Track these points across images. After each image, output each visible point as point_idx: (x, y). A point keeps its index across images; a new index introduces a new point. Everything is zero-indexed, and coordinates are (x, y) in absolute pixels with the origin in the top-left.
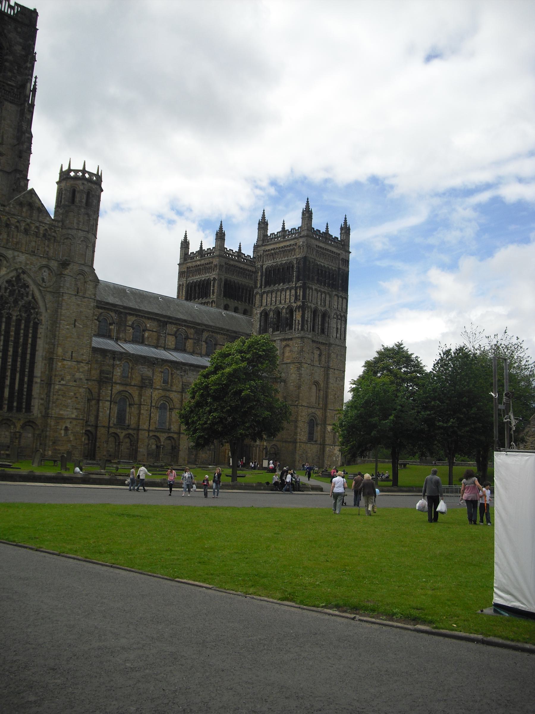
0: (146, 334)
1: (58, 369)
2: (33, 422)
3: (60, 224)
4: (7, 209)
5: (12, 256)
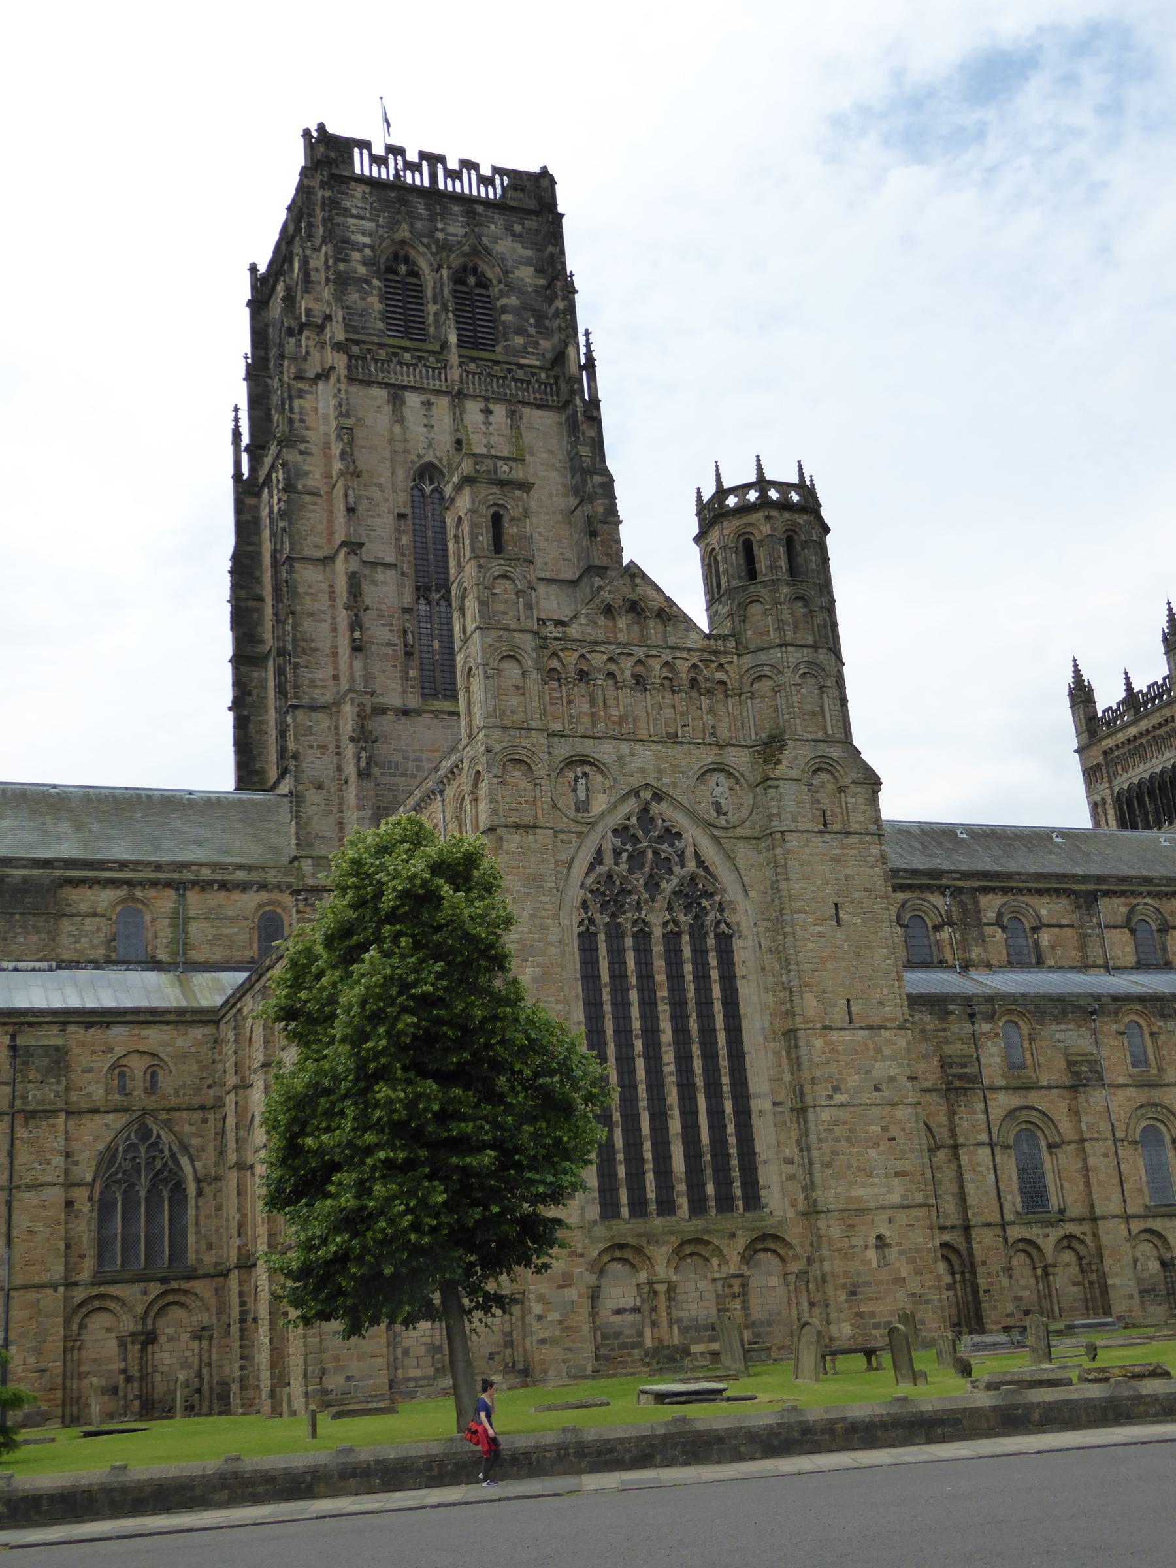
0: (1045, 938)
1: (816, 1060)
2: (776, 1238)
3: (731, 644)
5: (614, 757)
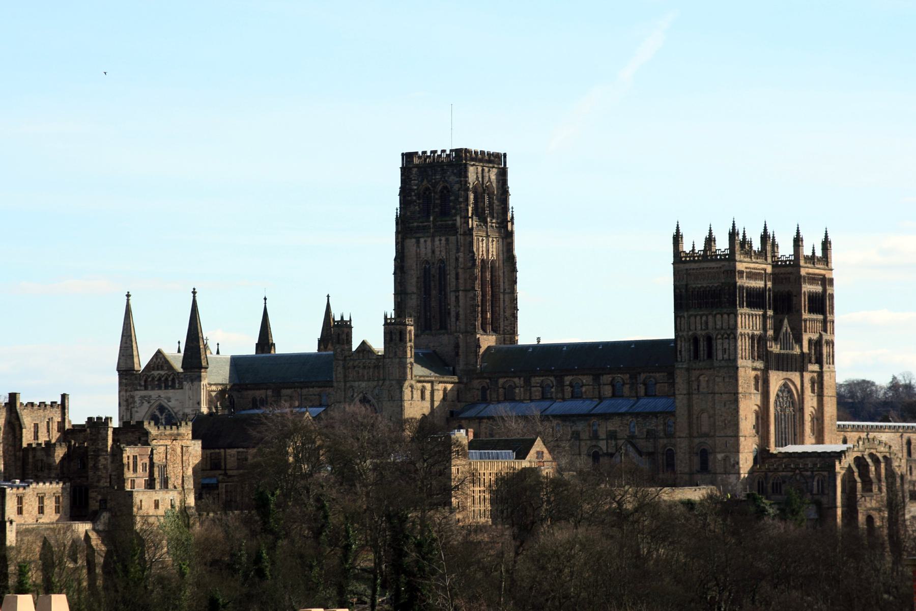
0: (584, 389)
4: (352, 357)
